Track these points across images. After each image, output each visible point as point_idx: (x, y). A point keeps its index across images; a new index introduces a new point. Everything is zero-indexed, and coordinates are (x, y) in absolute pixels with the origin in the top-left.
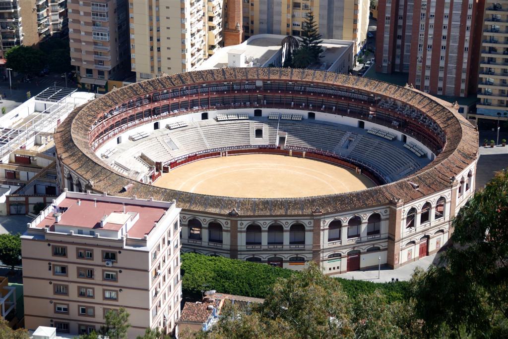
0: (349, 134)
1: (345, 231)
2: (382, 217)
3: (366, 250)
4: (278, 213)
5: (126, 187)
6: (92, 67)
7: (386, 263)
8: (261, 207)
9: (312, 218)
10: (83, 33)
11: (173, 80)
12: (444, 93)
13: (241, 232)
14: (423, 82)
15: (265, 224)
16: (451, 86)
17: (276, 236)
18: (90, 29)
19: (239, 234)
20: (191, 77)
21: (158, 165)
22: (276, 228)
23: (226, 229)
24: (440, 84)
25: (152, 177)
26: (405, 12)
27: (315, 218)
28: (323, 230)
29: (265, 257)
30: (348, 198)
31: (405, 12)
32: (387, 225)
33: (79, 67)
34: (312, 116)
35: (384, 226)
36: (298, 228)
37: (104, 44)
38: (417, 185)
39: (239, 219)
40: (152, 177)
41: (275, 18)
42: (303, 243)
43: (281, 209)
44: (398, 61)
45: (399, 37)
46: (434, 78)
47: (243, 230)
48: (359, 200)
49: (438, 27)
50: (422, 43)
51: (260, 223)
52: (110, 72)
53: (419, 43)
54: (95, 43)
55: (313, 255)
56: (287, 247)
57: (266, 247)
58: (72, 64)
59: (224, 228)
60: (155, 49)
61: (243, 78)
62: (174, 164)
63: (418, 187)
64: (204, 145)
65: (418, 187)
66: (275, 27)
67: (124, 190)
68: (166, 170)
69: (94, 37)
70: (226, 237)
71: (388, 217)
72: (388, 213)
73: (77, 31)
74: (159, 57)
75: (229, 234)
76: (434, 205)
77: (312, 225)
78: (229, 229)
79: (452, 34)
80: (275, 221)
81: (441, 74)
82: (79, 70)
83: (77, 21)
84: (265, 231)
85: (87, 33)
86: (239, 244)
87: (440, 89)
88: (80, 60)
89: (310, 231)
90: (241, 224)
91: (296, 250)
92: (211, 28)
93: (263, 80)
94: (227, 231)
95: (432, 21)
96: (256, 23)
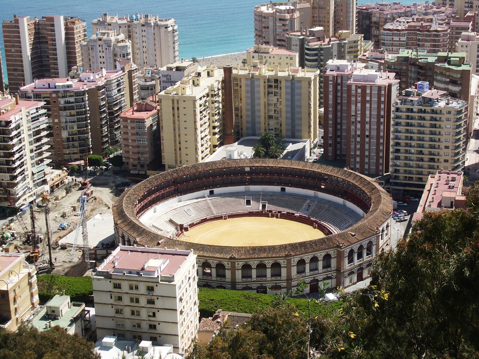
0: (308, 201)
1: (307, 267)
2: (332, 256)
4: (263, 256)
5: (160, 242)
8: (251, 252)
10: (130, 141)
11: (189, 169)
12: (369, 172)
13: (238, 269)
14: (355, 166)
15: (254, 264)
16: (373, 167)
17: (261, 271)
19: (236, 271)
21: (181, 227)
22: (261, 266)
23: (227, 268)
24: (366, 167)
25: (178, 235)
26: (341, 120)
27: (287, 258)
28: (294, 266)
29: (254, 286)
31: (341, 120)
32: (336, 261)
33: (128, 163)
34: (283, 190)
36: (276, 266)
37: (144, 147)
38: (354, 234)
39: (236, 261)
40: (178, 235)
41: (257, 125)
42: (280, 275)
43: (264, 253)
44: (338, 152)
45: (339, 137)
46: (362, 163)
47: (239, 268)
51: (251, 263)
52: (148, 165)
54: (138, 147)
55: (287, 284)
56: (270, 279)
57: (255, 279)
59: (226, 267)
60: (178, 149)
61: (237, 166)
62: (192, 225)
63: (355, 235)
64: (211, 211)
66: (257, 132)
67: (159, 244)
68: (186, 229)
69: (138, 143)
70: (228, 273)
71: (336, 256)
72: (336, 253)
74: (180, 154)
75: (230, 271)
77: (286, 263)
78: (230, 268)
79: (372, 134)
80: (261, 261)
81: (367, 160)
82: (128, 165)
84: (254, 269)
85: (132, 140)
88: (128, 158)
89: (285, 267)
90: (238, 264)
92: (215, 134)
93: (250, 167)
94: (228, 269)
96: (244, 129)
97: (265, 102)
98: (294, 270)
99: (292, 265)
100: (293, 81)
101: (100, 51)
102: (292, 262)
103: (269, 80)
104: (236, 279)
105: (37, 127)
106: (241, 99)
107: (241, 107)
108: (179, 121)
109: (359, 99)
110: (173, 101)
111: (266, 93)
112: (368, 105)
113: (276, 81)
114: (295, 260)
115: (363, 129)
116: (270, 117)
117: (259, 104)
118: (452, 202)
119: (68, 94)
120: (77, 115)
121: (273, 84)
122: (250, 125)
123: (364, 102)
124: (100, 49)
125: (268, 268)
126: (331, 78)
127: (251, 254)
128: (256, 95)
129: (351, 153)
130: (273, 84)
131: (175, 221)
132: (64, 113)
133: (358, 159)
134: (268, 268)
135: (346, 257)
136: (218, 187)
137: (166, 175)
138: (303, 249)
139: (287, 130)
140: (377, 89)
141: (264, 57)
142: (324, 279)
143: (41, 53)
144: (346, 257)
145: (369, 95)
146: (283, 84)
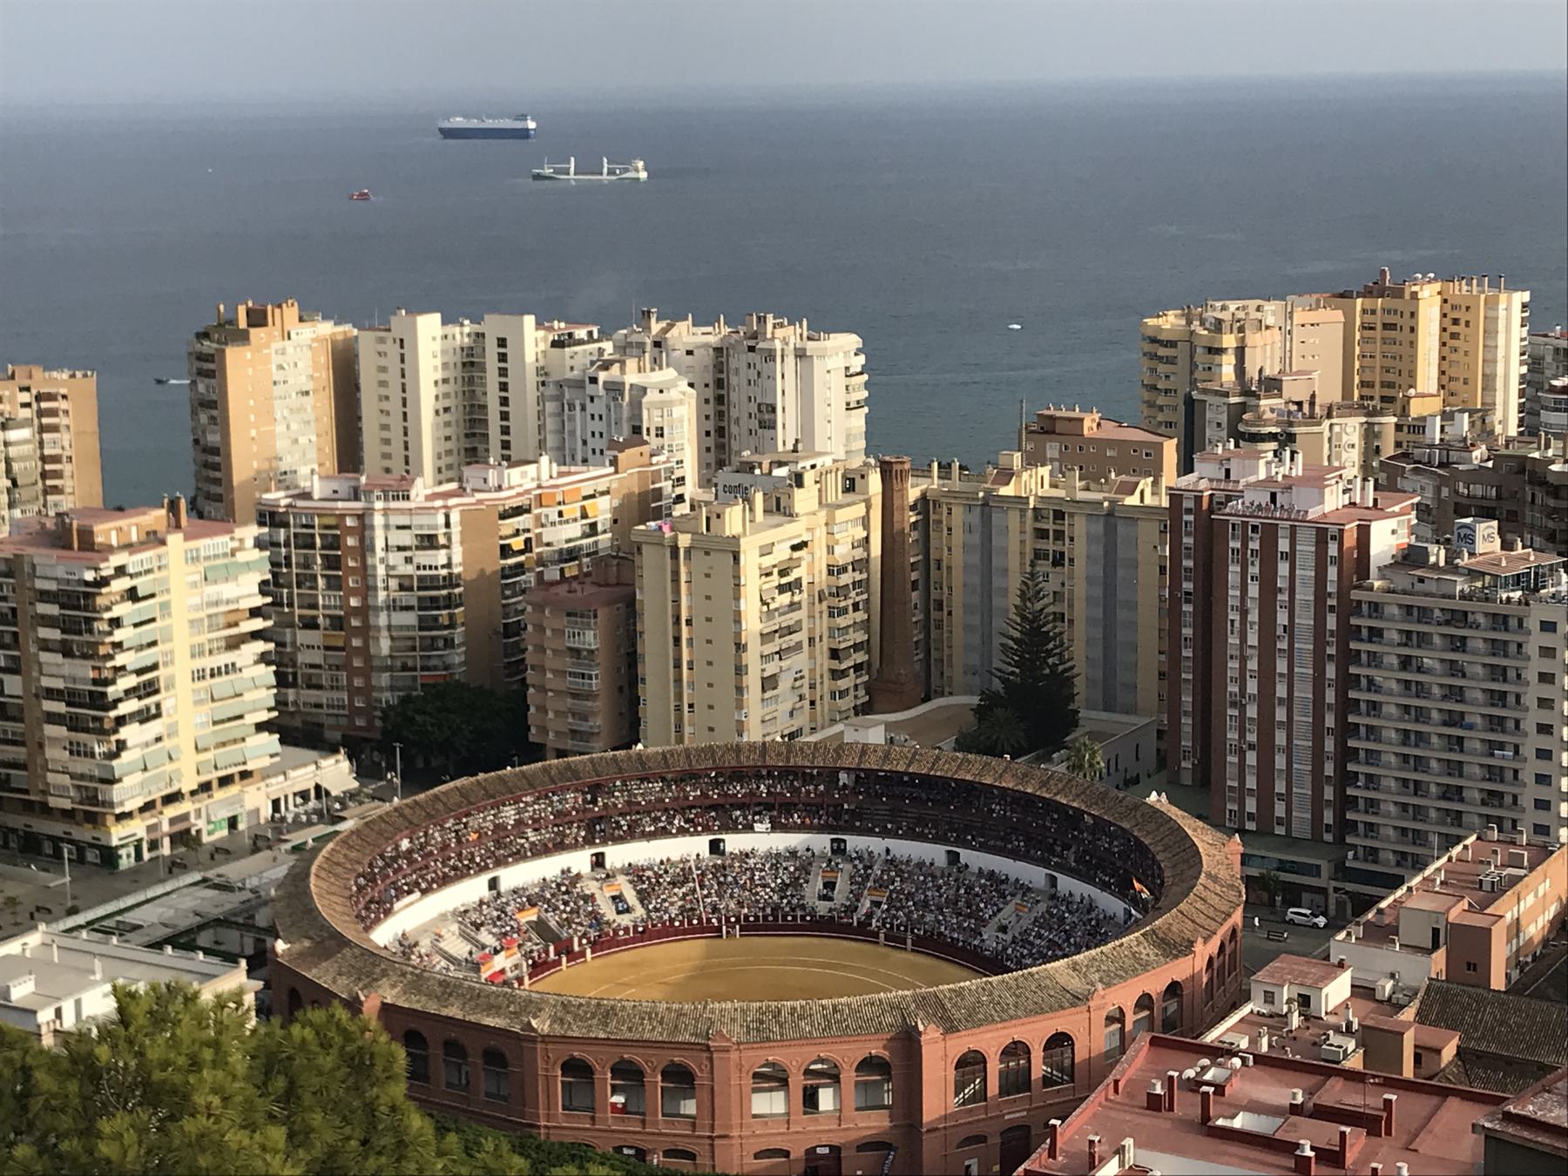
6: (569, 744)
10: (549, 675)
14: (1242, 805)
16: (1302, 815)
20: (688, 757)
24: (1280, 810)
37: (590, 696)
46: (1265, 795)
58: (531, 739)
73: (542, 669)
87: (1280, 822)
92: (836, 675)
95: (1253, 665)
100: (1112, 520)
111: (1029, 556)
113: (1059, 515)
115: (1267, 676)
118: (1436, 932)
120: (419, 589)
130: (1050, 526)
146: (1079, 527)
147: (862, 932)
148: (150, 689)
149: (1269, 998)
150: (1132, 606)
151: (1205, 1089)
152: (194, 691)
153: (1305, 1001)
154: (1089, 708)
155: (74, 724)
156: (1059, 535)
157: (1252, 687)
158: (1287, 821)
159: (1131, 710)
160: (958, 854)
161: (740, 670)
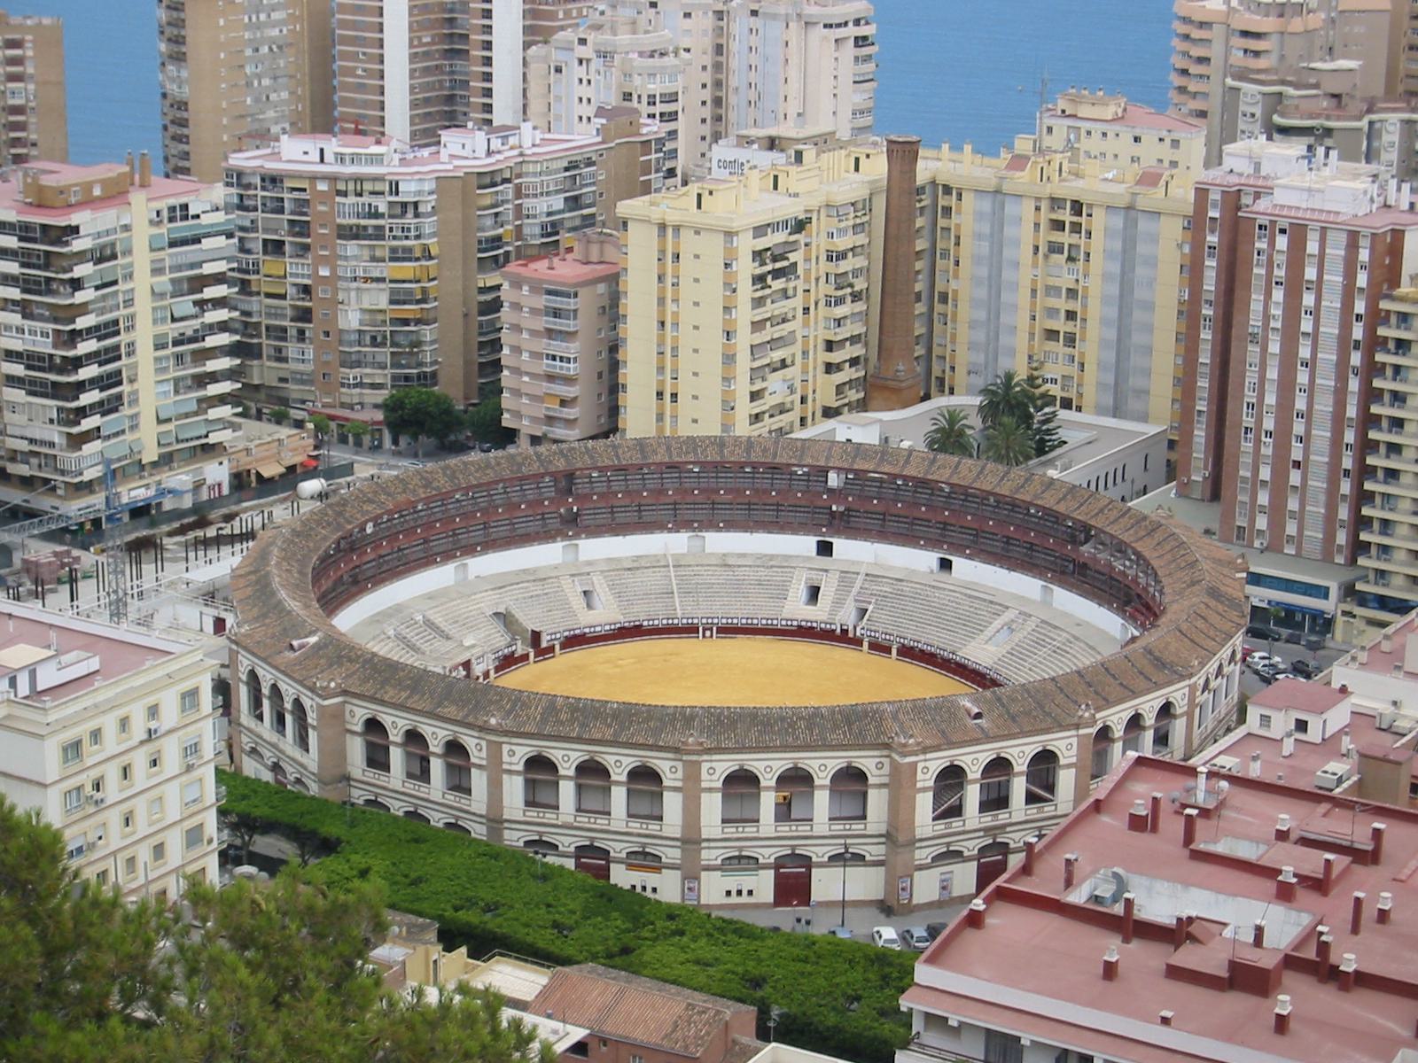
0: (1009, 615)
2: (871, 780)
3: (826, 859)
4: (599, 736)
5: (295, 643)
7: (881, 897)
8: (563, 717)
9: (679, 756)
10: (525, 356)
11: (620, 451)
12: (1298, 555)
13: (510, 772)
14: (1252, 521)
18: (543, 345)
19: (505, 776)
24: (1291, 528)
25: (508, 662)
27: (685, 758)
28: (710, 790)
29: (568, 843)
30: (783, 719)
35: (877, 802)
40: (508, 662)
43: (610, 726)
48: (810, 728)
49: (1287, 386)
50: (1248, 421)
53: (1244, 424)
54: (551, 378)
56: (621, 827)
57: (571, 819)
58: (504, 424)
59: (473, 760)
62: (575, 641)
63: (978, 716)
65: (978, 716)
69: (548, 366)
70: (478, 780)
71: (885, 780)
72: (886, 770)
73: (517, 350)
74: (675, 417)
76: (1020, 765)
77: (680, 775)
78: (484, 763)
79: (1316, 407)
81: (1293, 504)
83: (517, 328)
86: (506, 802)
87: (1290, 539)
88: (518, 415)
89: (675, 789)
91: (639, 835)
92: (830, 368)
94: (480, 767)
95: (1272, 374)
96: (961, 371)
97: (1034, 282)
98: (712, 807)
99: (704, 785)
100: (1132, 213)
101: (581, 81)
102: (704, 775)
103: (1056, 203)
104: (501, 808)
105: (192, 266)
106: (957, 263)
107: (955, 292)
108: (675, 301)
109: (1280, 273)
110: (663, 227)
112: (1308, 300)
113: (1077, 207)
114: (718, 767)
116: (1052, 334)
117: (1015, 287)
119: (368, 186)
121: (1066, 216)
122: (981, 358)
123: (1294, 286)
124: (580, 72)
125: (618, 783)
126: (1215, 196)
127: (562, 723)
128: (1008, 253)
129: (1241, 473)
130: (1066, 216)
131: (521, 620)
132: (352, 248)
133: (1263, 498)
134: (618, 783)
135: (924, 790)
136: (719, 530)
137: (526, 458)
138: (753, 734)
139: (1101, 386)
140: (1343, 238)
141: (1083, 133)
142: (836, 859)
143: (452, 88)
144: (924, 790)
145: (1316, 260)
146: (1098, 221)
147: (843, 638)
148: (112, 355)
149: (1265, 720)
150: (1149, 307)
151: (1188, 811)
152: (157, 359)
153: (1302, 726)
154: (1100, 411)
155: (35, 388)
156: (1076, 228)
157: (1271, 399)
158: (1298, 540)
159: (1144, 418)
160: (950, 562)
161: (729, 359)
